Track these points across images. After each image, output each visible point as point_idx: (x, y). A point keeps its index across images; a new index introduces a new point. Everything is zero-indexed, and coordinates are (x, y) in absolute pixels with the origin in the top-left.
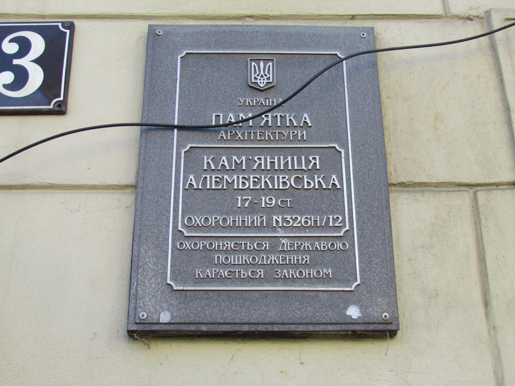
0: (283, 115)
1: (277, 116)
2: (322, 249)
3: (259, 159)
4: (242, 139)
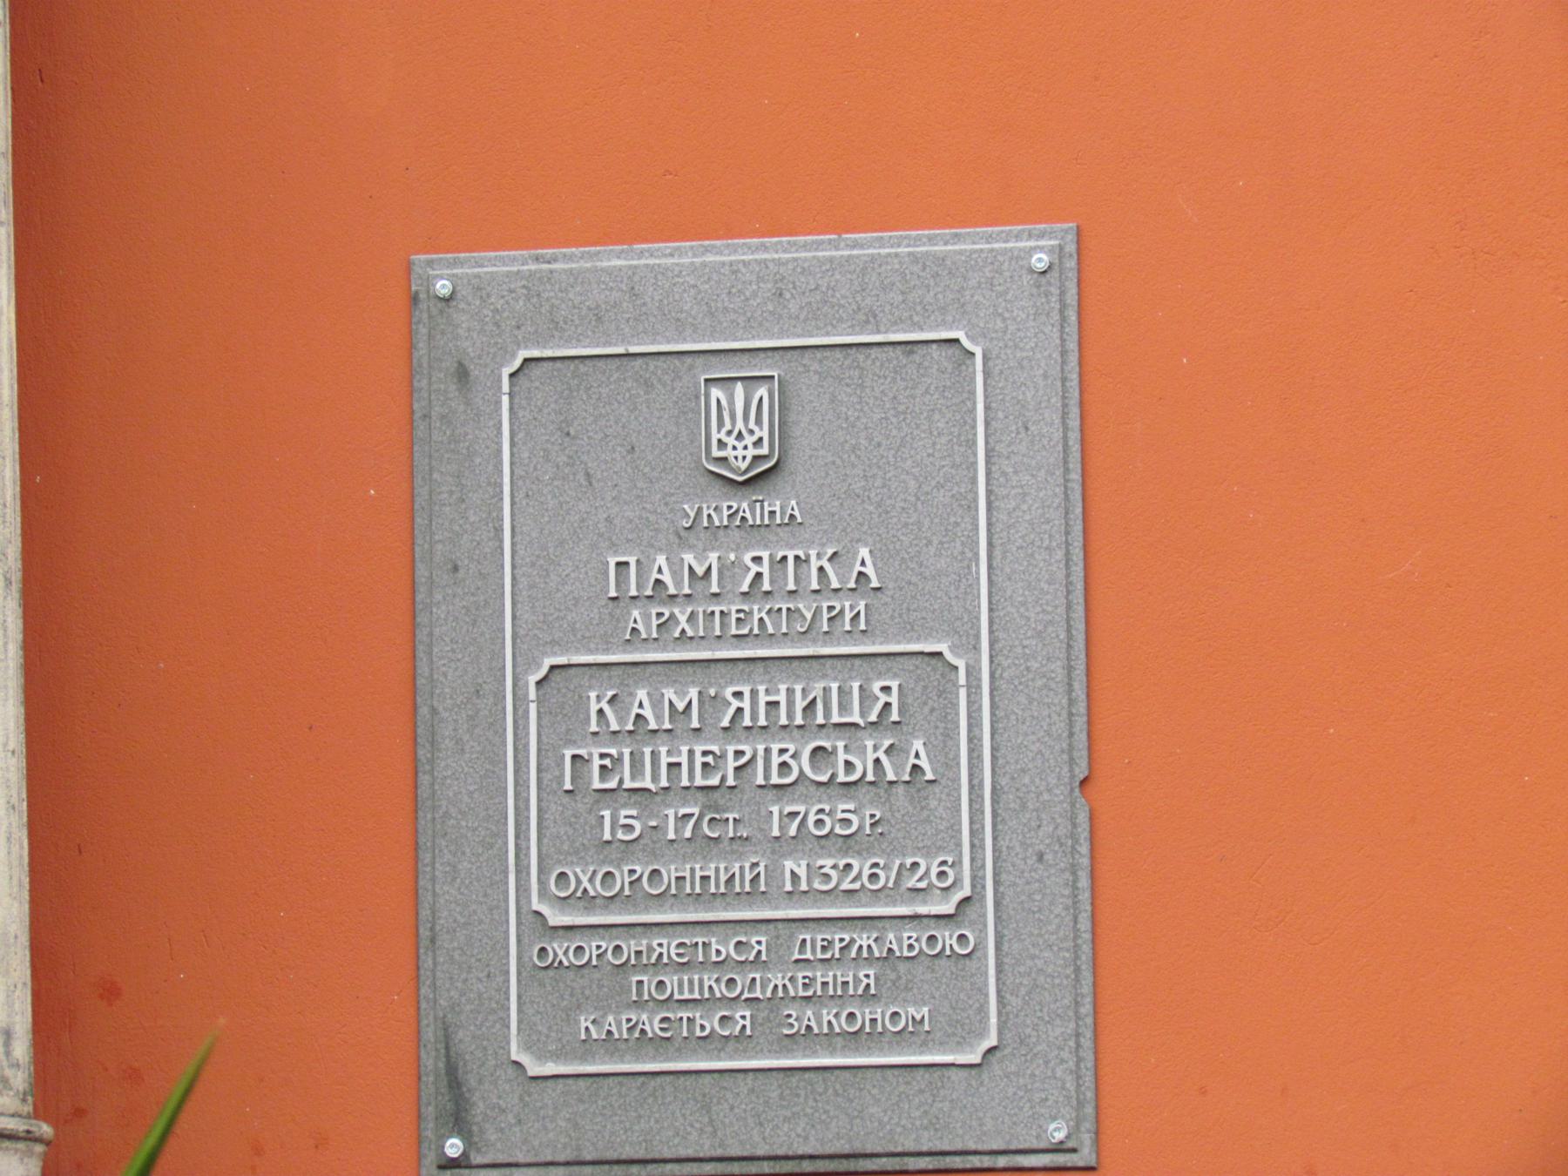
0: (801, 554)
1: (784, 558)
2: (906, 953)
4: (690, 633)
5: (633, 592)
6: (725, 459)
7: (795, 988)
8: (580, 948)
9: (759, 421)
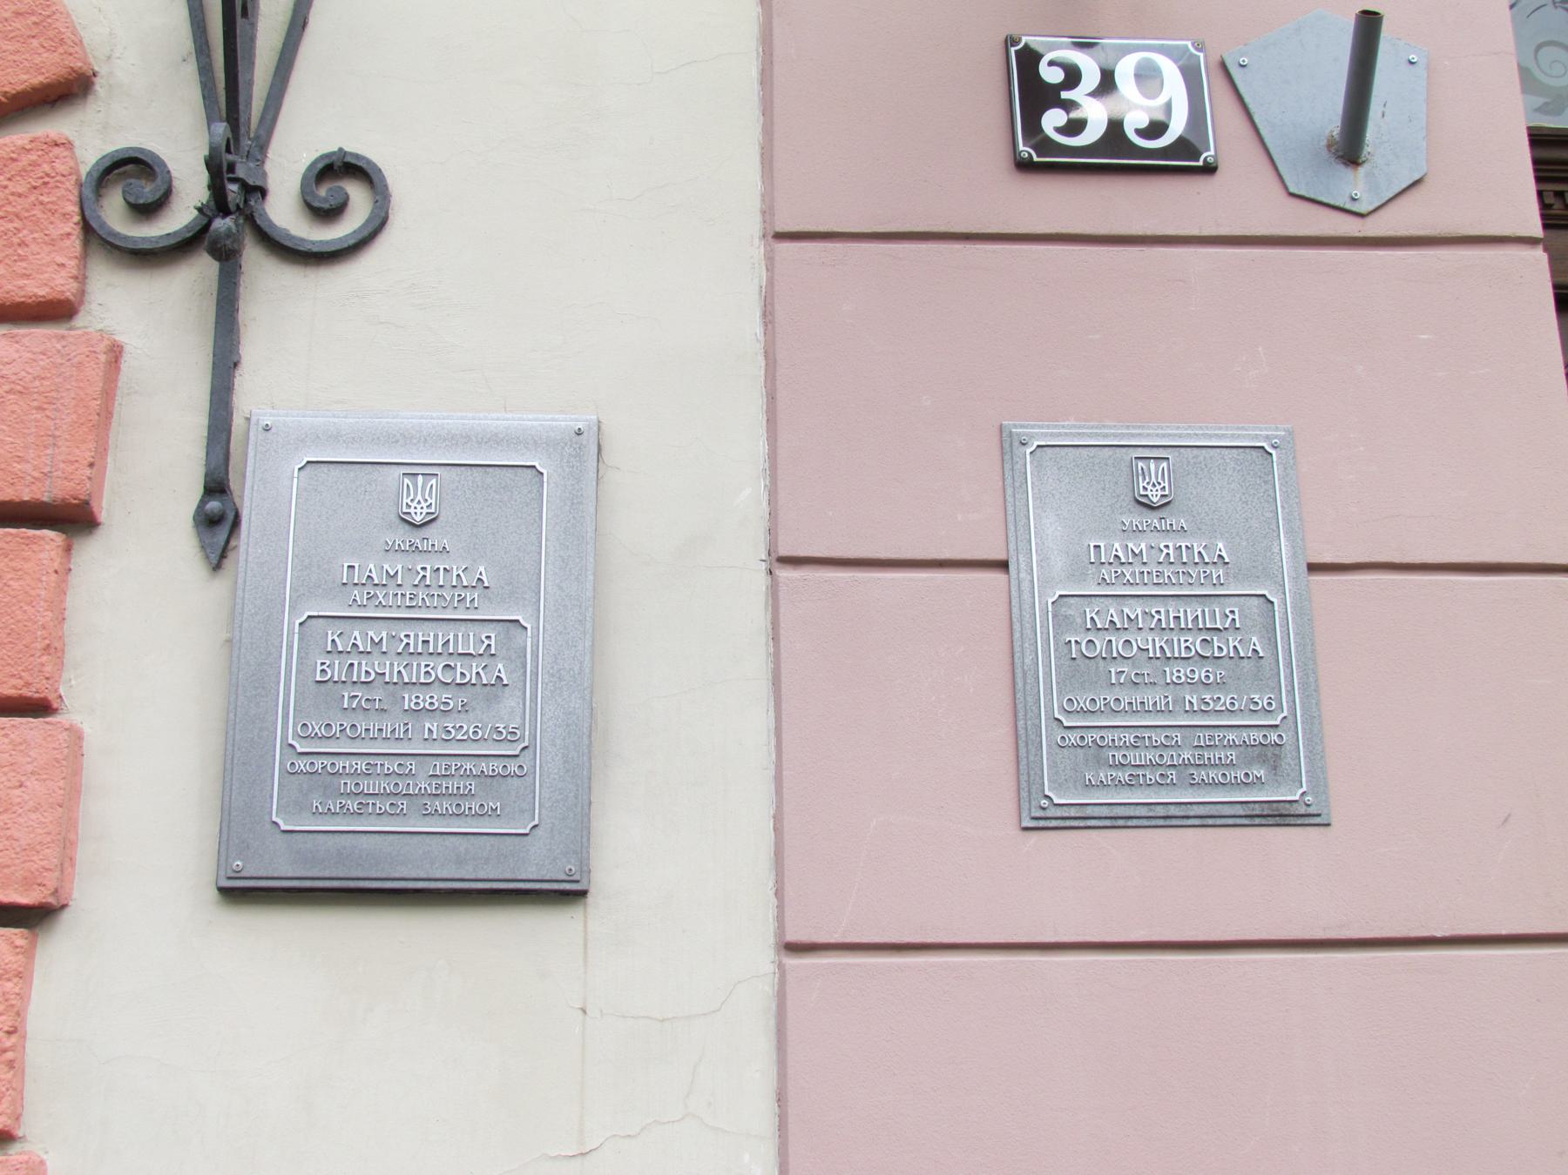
0: (447, 567)
1: (438, 569)
2: (491, 774)
5: (356, 581)
6: (409, 513)
7: (431, 790)
8: (333, 764)
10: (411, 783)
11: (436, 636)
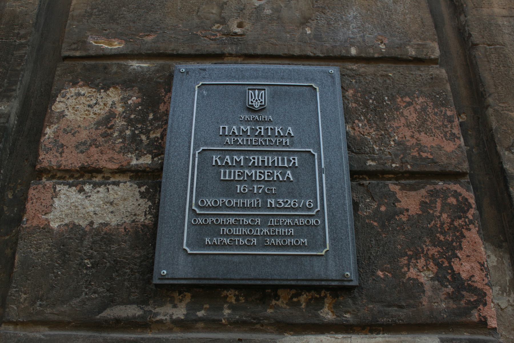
0: (272, 127)
1: (268, 128)
2: (300, 224)
3: (254, 158)
4: (242, 144)
6: (252, 105)
7: (270, 233)
9: (262, 98)
10: (259, 229)
11: (268, 159)
